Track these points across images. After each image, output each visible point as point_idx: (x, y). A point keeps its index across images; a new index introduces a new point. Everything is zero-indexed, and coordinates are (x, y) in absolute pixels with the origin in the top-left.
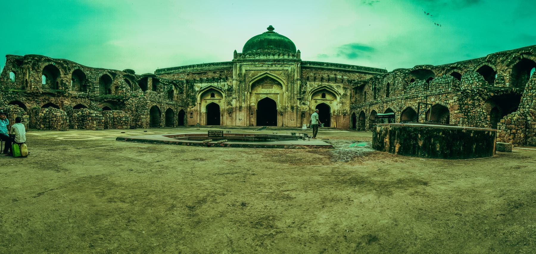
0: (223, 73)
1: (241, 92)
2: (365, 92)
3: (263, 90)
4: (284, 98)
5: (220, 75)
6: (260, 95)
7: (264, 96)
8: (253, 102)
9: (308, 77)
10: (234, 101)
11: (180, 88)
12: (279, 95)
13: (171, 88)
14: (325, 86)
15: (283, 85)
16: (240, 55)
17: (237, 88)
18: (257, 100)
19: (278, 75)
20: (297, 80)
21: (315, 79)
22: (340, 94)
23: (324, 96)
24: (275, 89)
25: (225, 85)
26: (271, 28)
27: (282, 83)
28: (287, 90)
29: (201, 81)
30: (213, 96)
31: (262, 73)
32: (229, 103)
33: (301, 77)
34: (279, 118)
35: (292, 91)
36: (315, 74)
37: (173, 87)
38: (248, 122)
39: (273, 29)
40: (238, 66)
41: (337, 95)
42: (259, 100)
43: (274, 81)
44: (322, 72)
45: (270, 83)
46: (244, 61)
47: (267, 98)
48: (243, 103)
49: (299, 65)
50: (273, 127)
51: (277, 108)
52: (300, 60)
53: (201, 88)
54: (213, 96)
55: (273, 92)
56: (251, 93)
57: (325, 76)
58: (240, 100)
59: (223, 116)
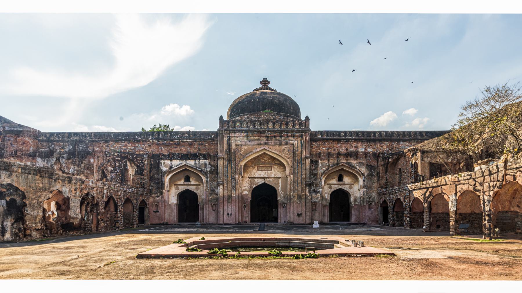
0: (202, 148)
1: (229, 176)
2: (400, 170)
3: (260, 172)
4: (289, 184)
5: (199, 150)
6: (256, 180)
7: (260, 182)
8: (245, 188)
9: (320, 154)
10: (220, 189)
11: (138, 166)
12: (280, 180)
13: (126, 165)
14: (342, 165)
15: (287, 166)
16: (228, 122)
17: (225, 169)
18: (251, 187)
19: (280, 152)
20: (306, 157)
21: (329, 155)
22: (363, 175)
23: (340, 179)
24: (275, 172)
25: (205, 164)
26: (265, 82)
27: (285, 163)
28: (293, 173)
29: (171, 157)
30: (187, 179)
31: (258, 150)
32: (213, 191)
33: (311, 155)
34: (281, 211)
35: (299, 174)
36: (328, 149)
37: (128, 164)
38: (240, 218)
39: (269, 83)
40: (226, 139)
41: (359, 177)
42: (254, 186)
43: (274, 159)
44: (340, 145)
45: (268, 163)
46: (234, 131)
47: (264, 184)
48: (233, 192)
49: (308, 138)
50: (273, 224)
51: (279, 198)
52: (310, 130)
53: (171, 167)
54: (187, 179)
55: (273, 176)
56: (242, 177)
57: (343, 150)
58: (229, 187)
59: (203, 209)
